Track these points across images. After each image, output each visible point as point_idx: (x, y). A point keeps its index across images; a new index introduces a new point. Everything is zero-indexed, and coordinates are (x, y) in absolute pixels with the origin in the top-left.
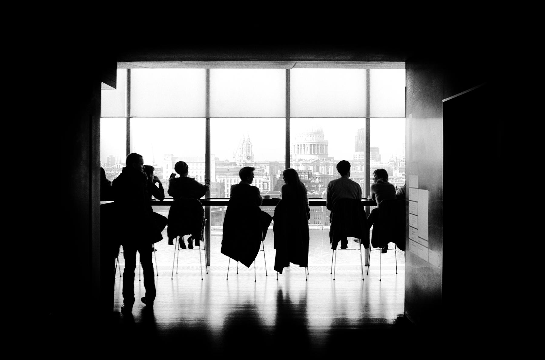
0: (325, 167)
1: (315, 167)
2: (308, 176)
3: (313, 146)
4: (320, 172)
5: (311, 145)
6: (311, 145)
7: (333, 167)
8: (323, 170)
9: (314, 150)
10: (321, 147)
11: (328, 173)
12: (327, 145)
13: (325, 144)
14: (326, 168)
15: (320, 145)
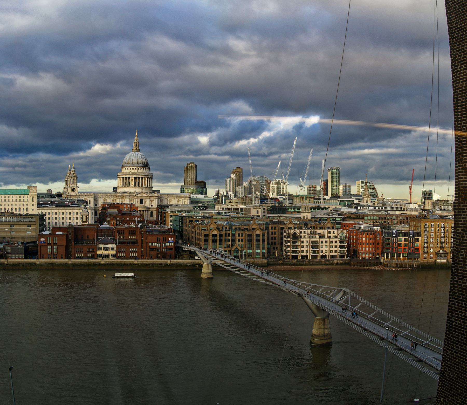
0: (149, 200)
1: (139, 200)
2: (130, 208)
3: (137, 178)
4: (144, 204)
5: (135, 178)
6: (135, 178)
7: (156, 200)
8: (147, 203)
9: (139, 183)
10: (145, 180)
11: (152, 206)
12: (152, 178)
13: (150, 177)
14: (150, 200)
15: (145, 178)
